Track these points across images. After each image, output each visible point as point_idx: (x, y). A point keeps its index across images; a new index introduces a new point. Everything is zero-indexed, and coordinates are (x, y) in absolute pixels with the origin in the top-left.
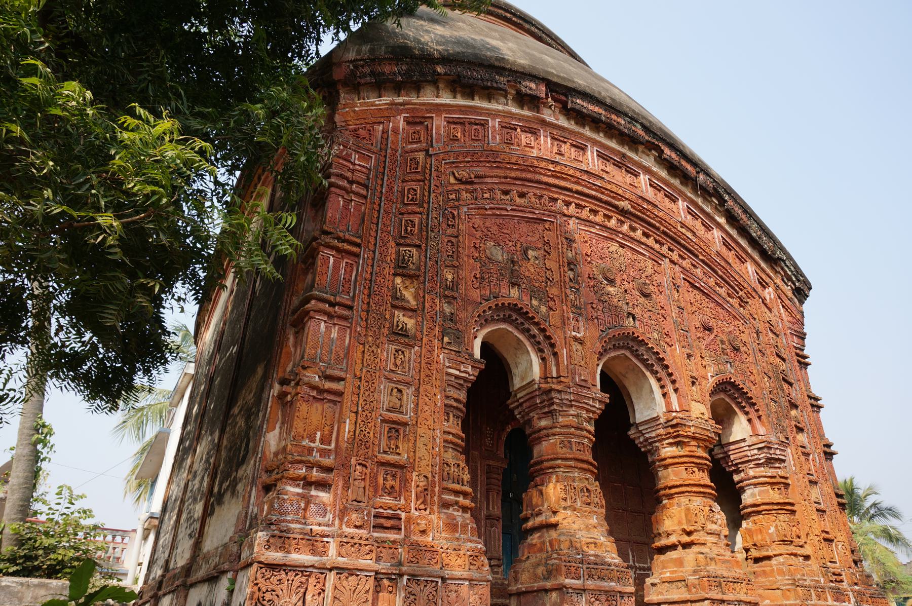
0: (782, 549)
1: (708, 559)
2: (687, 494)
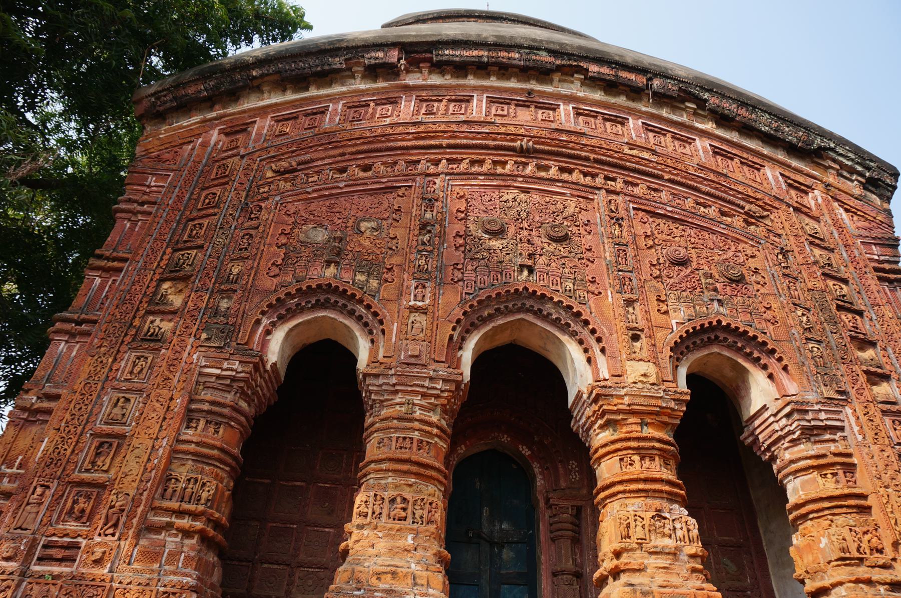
0: (843, 573)
1: (638, 593)
2: (620, 496)
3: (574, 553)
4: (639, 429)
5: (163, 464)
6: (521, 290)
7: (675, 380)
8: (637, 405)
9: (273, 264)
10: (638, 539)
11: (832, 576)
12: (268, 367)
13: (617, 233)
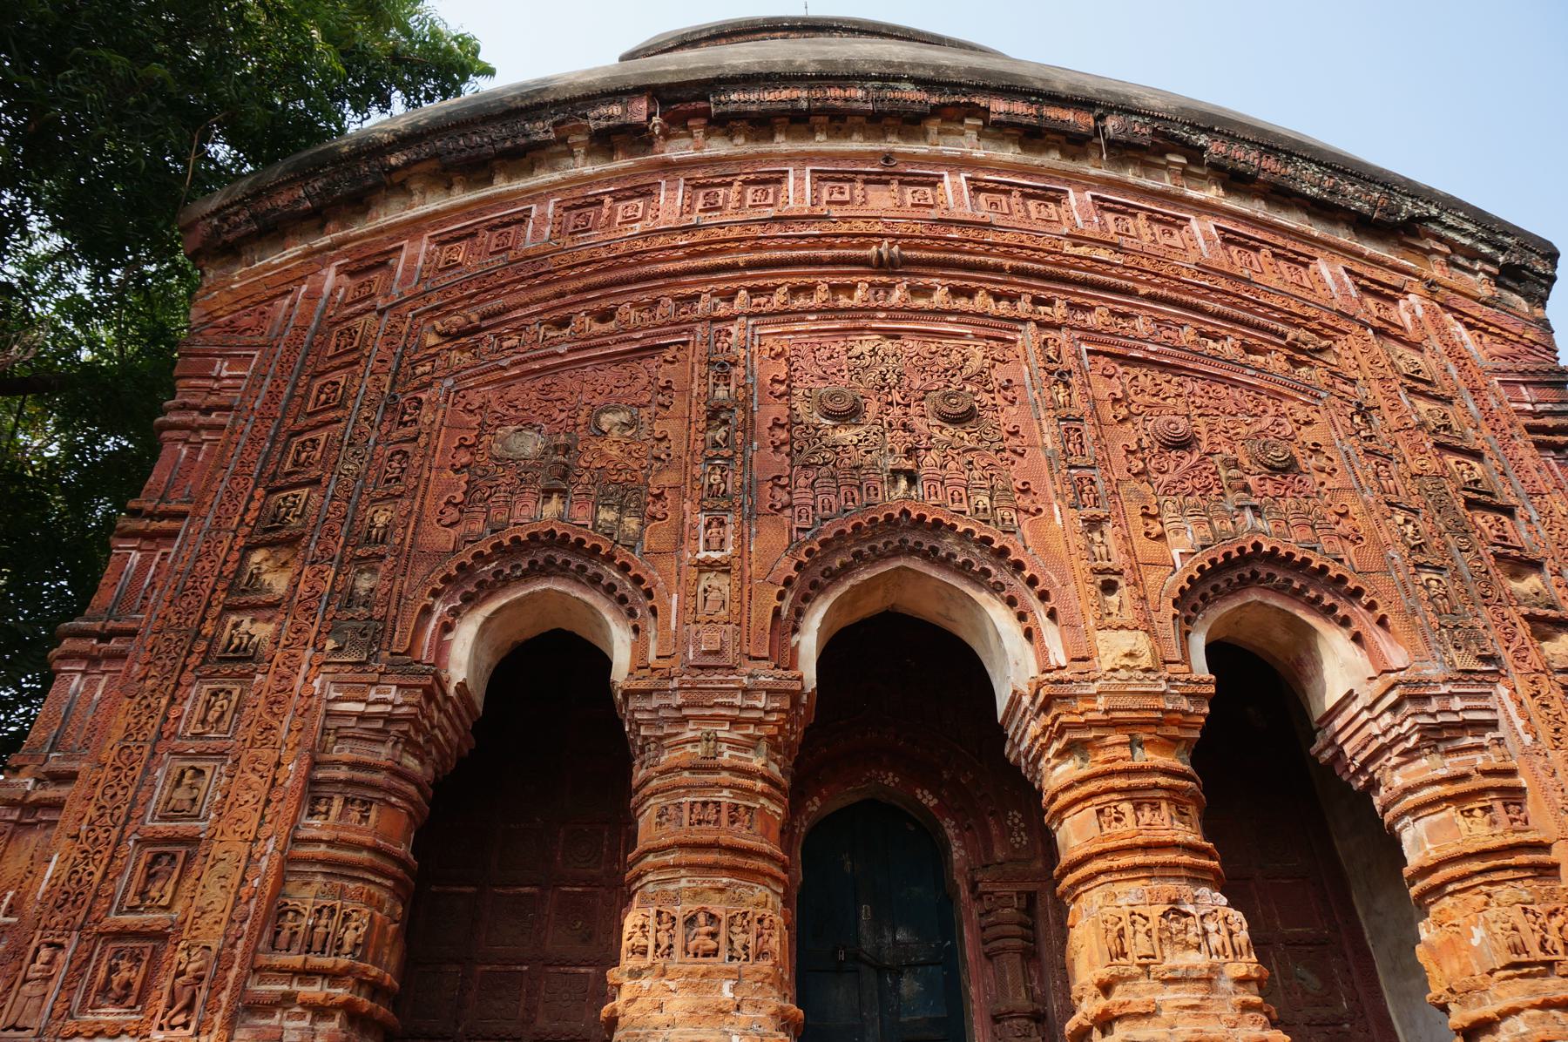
0: (1516, 992)
2: (1102, 878)
3: (1027, 977)
4: (1127, 753)
5: (269, 887)
6: (897, 516)
7: (1186, 659)
8: (1120, 710)
9: (448, 503)
10: (1140, 958)
11: (1499, 997)
12: (451, 691)
13: (1061, 400)
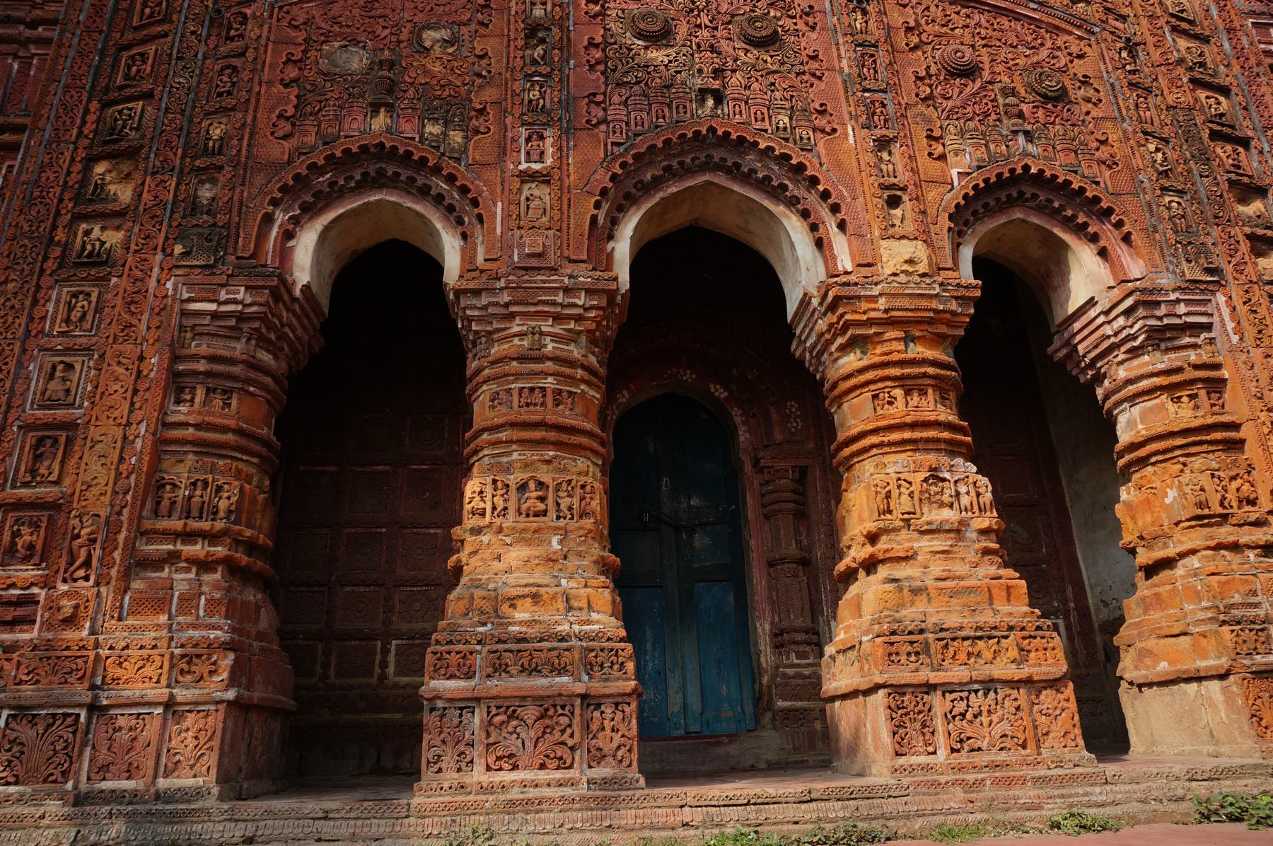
0: (1197, 538)
1: (905, 591)
2: (875, 451)
3: (797, 533)
4: (902, 347)
5: (146, 464)
6: (704, 132)
7: (956, 267)
8: (898, 310)
9: (280, 116)
10: (903, 514)
11: (1181, 542)
12: (297, 293)
13: (858, 26)
